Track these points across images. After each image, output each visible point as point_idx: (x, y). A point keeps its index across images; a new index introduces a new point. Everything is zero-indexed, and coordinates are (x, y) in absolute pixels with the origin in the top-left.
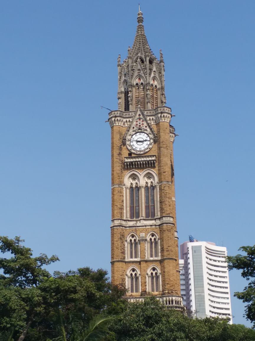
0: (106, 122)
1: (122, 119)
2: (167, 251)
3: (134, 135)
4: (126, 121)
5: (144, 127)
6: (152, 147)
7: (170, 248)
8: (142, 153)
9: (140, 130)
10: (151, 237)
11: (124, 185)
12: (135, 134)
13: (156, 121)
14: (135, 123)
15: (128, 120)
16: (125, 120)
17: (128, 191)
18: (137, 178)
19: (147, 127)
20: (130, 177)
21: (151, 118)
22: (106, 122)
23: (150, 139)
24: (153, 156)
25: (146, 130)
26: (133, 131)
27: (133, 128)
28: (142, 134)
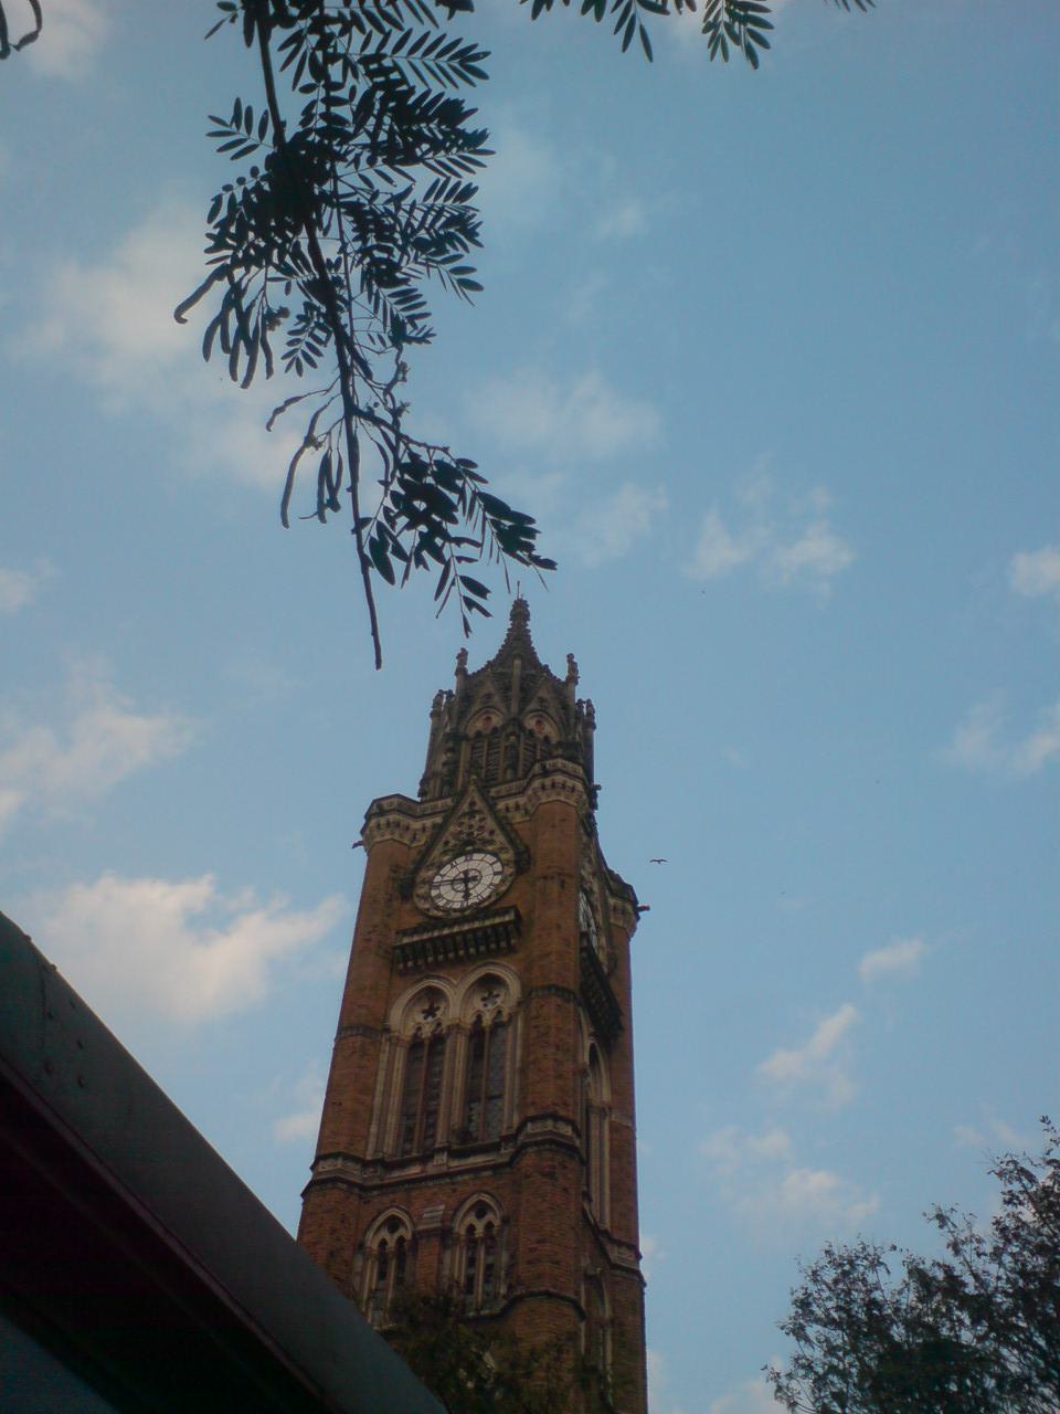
0: (355, 845)
1: (405, 820)
2: (529, 1262)
3: (449, 866)
4: (424, 829)
5: (486, 835)
6: (508, 891)
7: (548, 1246)
8: (467, 913)
9: (467, 847)
10: (471, 1219)
11: (387, 1030)
12: (449, 862)
13: (529, 807)
14: (452, 828)
15: (428, 822)
16: (416, 825)
17: (401, 1054)
18: (442, 1006)
19: (498, 831)
20: (417, 998)
21: (511, 802)
22: (355, 845)
23: (503, 865)
24: (506, 911)
25: (491, 842)
26: (445, 853)
27: (447, 843)
28: (476, 856)
